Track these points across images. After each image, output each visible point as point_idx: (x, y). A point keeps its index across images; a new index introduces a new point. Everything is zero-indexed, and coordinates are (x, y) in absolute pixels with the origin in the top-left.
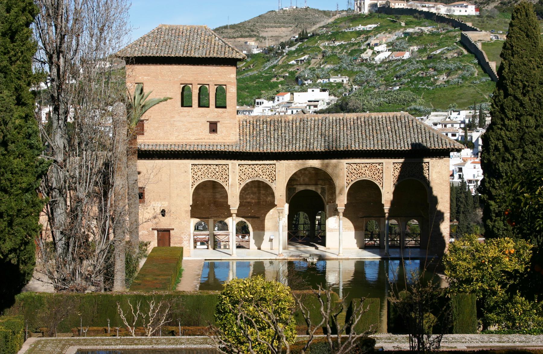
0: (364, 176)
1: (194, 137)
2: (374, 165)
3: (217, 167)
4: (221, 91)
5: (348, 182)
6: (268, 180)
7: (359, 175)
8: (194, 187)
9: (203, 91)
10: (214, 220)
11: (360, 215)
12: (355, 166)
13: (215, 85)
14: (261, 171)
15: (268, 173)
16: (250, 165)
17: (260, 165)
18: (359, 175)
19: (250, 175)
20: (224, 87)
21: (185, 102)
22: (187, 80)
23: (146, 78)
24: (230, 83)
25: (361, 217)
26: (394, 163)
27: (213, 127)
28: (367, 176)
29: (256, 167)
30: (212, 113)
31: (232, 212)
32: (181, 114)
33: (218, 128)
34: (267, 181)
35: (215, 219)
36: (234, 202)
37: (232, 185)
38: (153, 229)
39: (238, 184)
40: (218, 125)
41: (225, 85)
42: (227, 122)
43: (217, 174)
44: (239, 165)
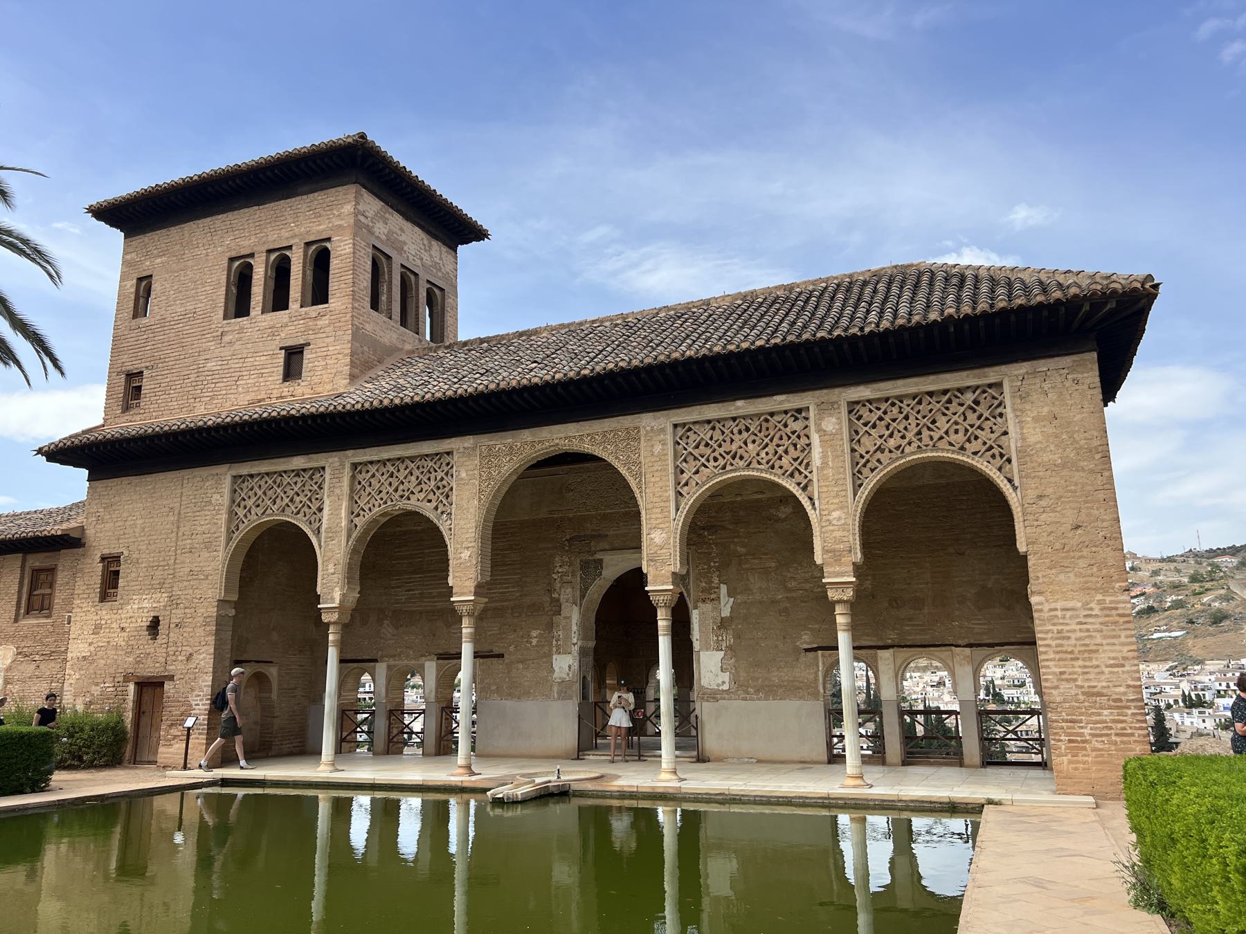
0: (741, 463)
1: (248, 398)
2: (773, 420)
3: (299, 480)
4: (321, 260)
5: (684, 491)
6: (434, 504)
7: (721, 462)
8: (233, 545)
9: (281, 271)
10: (389, 667)
11: (806, 640)
12: (704, 433)
13: (308, 244)
14: (413, 478)
15: (433, 483)
16: (384, 463)
17: (412, 459)
18: (721, 462)
19: (383, 495)
20: (328, 245)
21: (239, 305)
22: (245, 246)
23: (159, 260)
24: (340, 226)
25: (807, 650)
26: (852, 405)
27: (293, 359)
28: (755, 464)
29: (402, 467)
30: (295, 321)
31: (325, 618)
32: (227, 338)
33: (305, 362)
34: (427, 510)
35: (392, 662)
36: (333, 589)
37: (329, 529)
38: (127, 679)
39: (344, 523)
40: (308, 355)
41: (329, 239)
42: (327, 340)
43: (297, 499)
44: (355, 466)
